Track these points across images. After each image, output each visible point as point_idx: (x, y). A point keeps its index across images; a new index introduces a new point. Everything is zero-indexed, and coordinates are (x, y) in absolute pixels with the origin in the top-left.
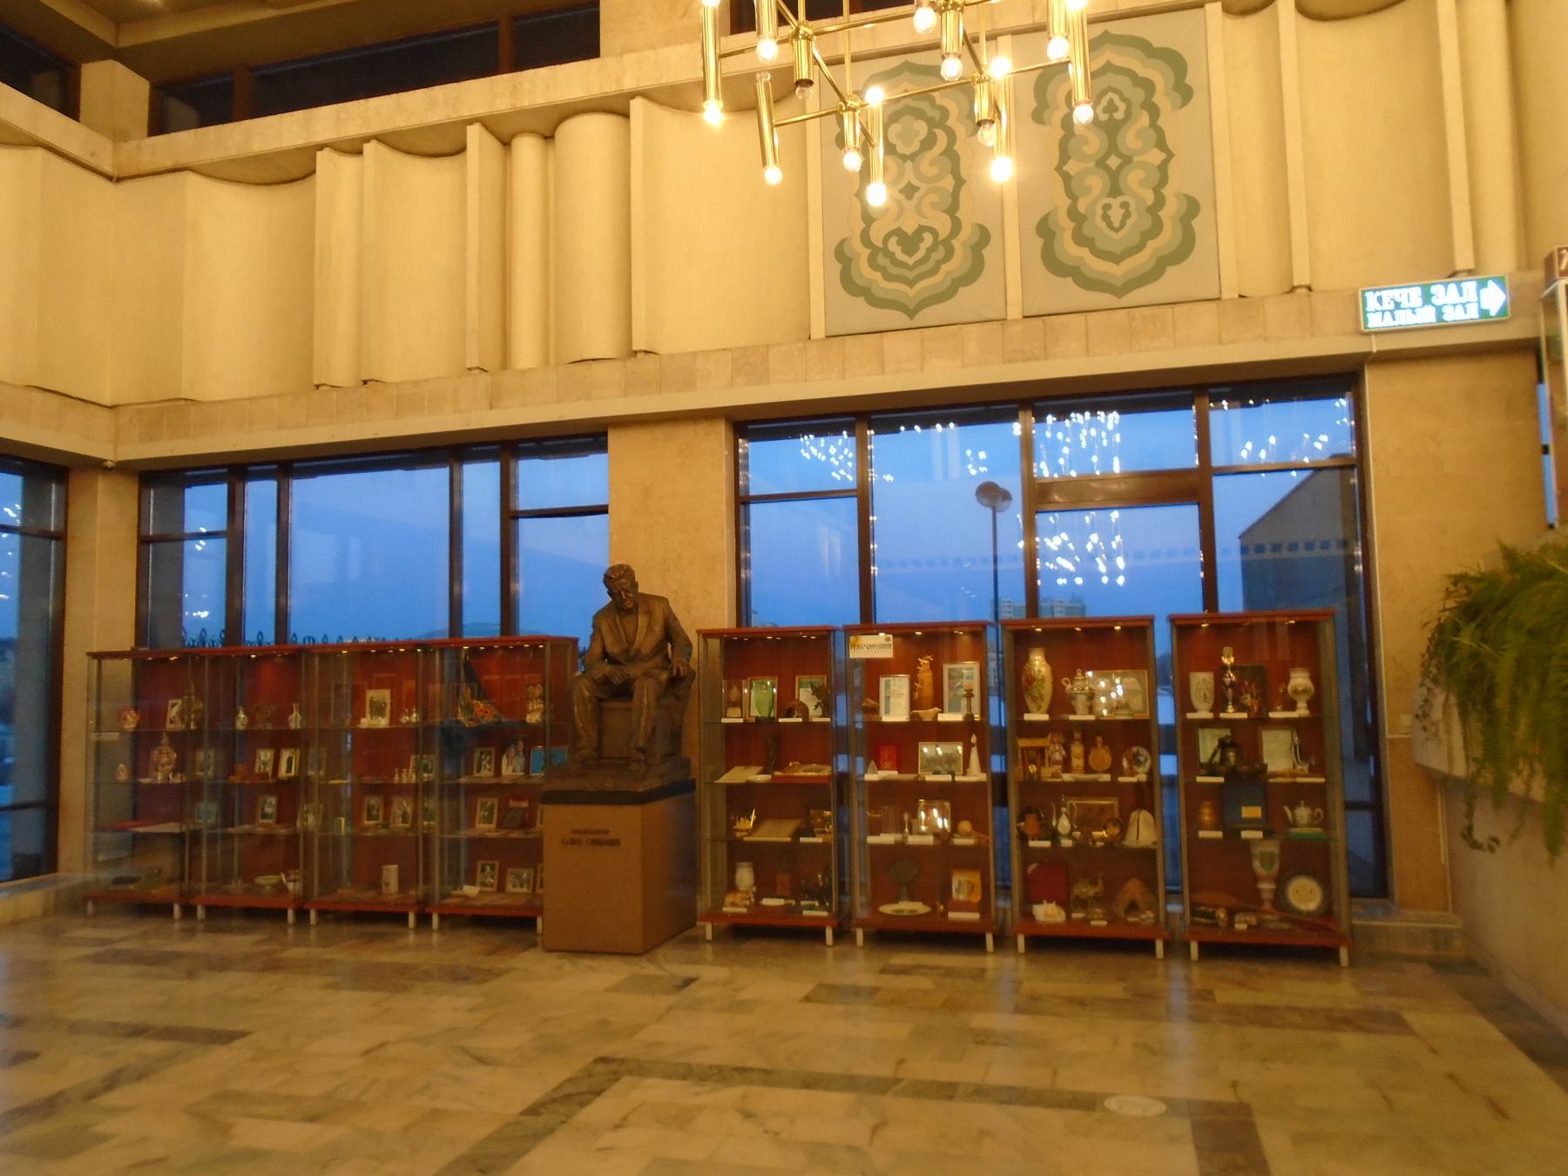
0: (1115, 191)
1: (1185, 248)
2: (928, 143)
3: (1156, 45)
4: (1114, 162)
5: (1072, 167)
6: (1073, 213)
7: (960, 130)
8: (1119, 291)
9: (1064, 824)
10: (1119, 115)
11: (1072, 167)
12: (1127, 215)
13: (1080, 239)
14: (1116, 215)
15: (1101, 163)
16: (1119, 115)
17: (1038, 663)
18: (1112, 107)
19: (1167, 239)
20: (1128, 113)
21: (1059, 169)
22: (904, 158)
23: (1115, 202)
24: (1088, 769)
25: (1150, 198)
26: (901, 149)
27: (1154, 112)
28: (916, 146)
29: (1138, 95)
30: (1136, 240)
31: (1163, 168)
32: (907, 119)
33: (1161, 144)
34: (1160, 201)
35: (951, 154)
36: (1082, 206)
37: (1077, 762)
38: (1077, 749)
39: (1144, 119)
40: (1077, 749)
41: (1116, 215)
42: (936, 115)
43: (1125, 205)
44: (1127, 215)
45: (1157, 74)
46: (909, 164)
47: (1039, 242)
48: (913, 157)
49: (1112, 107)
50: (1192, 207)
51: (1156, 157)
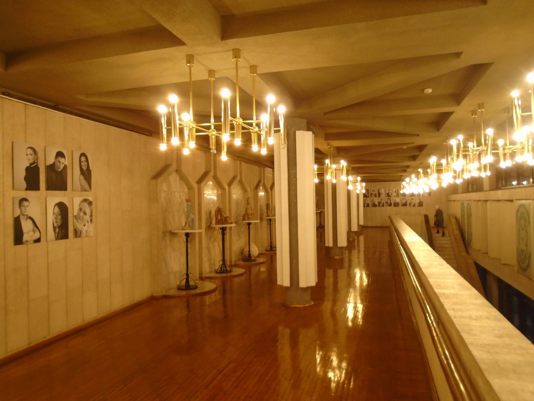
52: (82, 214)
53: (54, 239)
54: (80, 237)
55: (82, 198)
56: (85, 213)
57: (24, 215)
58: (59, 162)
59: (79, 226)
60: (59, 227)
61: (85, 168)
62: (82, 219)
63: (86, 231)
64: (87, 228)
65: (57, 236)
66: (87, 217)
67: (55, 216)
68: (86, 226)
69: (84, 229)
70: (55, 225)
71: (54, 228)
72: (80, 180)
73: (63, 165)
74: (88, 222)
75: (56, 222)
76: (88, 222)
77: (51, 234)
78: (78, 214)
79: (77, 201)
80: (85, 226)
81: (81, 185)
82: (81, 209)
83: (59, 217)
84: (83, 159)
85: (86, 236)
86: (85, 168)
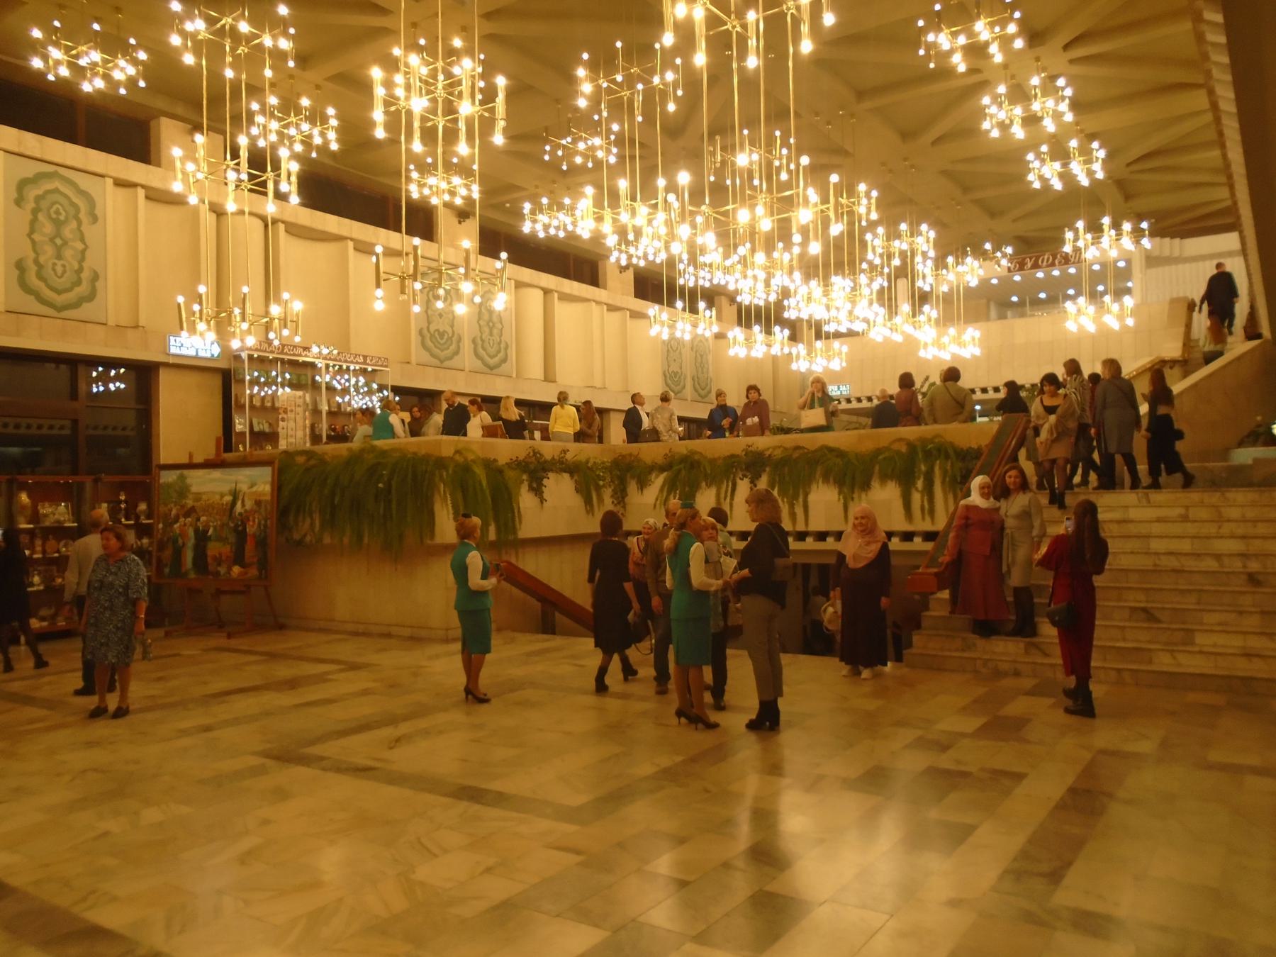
0: (59, 257)
1: (91, 297)
4: (59, 241)
5: (36, 237)
6: (36, 262)
8: (60, 309)
9: (36, 579)
11: (36, 237)
12: (64, 272)
13: (40, 277)
14: (59, 269)
15: (52, 240)
16: (62, 218)
17: (24, 497)
19: (83, 289)
20: (67, 218)
21: (29, 235)
23: (59, 263)
24: (44, 552)
25: (76, 266)
27: (80, 223)
29: (72, 211)
30: (68, 285)
31: (83, 252)
33: (82, 240)
34: (80, 270)
36: (42, 259)
37: (39, 549)
38: (38, 542)
39: (74, 224)
40: (38, 542)
41: (59, 269)
43: (64, 266)
44: (64, 272)
47: (17, 272)
49: (58, 212)
50: (95, 277)
51: (80, 246)
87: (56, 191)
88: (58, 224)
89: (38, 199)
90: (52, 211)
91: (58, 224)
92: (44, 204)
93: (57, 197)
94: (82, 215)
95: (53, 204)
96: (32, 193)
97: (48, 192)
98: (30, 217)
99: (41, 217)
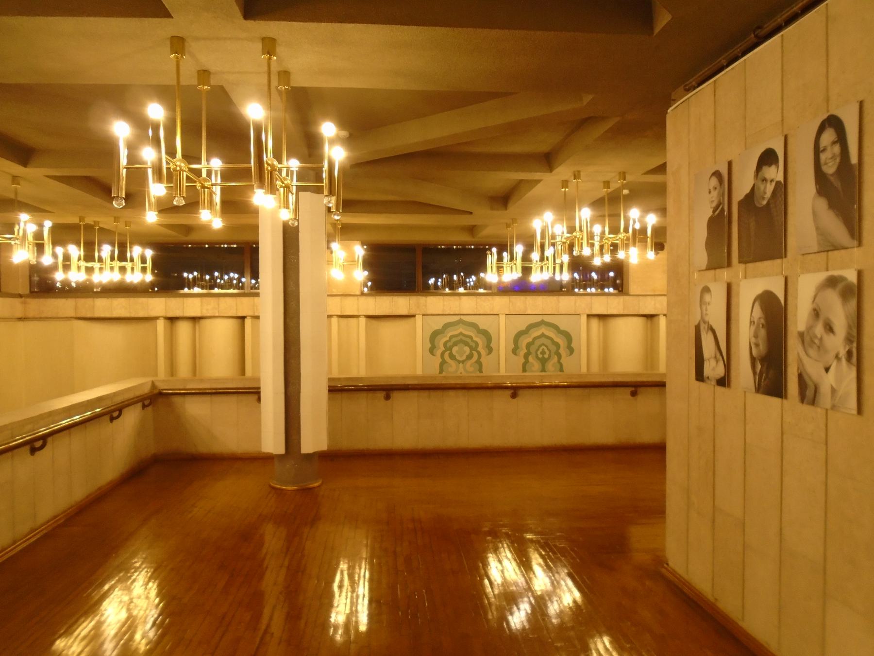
2: (470, 357)
3: (562, 328)
7: (483, 352)
10: (546, 356)
16: (546, 356)
18: (543, 353)
20: (550, 356)
22: (459, 362)
26: (458, 358)
28: (464, 357)
29: (553, 348)
32: (461, 345)
35: (479, 363)
39: (556, 358)
42: (474, 345)
45: (561, 340)
46: (461, 365)
48: (463, 362)
49: (543, 353)
52: (819, 330)
53: (754, 389)
54: (813, 402)
55: (822, 276)
56: (829, 328)
57: (705, 322)
58: (764, 180)
59: (813, 370)
60: (763, 360)
61: (830, 169)
62: (821, 347)
63: (834, 391)
64: (837, 380)
65: (759, 385)
66: (837, 343)
67: (753, 328)
68: (832, 370)
69: (828, 381)
70: (755, 352)
71: (753, 360)
72: (814, 213)
73: (774, 184)
74: (837, 357)
75: (757, 345)
76: (837, 357)
77: (744, 372)
78: (810, 328)
79: (807, 286)
80: (827, 370)
81: (820, 231)
82: (816, 313)
83: (763, 333)
84: (829, 136)
85: (834, 407)
86: (830, 169)
87: (543, 335)
88: (543, 362)
89: (529, 345)
90: (539, 353)
91: (543, 362)
92: (533, 349)
93: (543, 340)
94: (563, 351)
95: (540, 346)
96: (525, 341)
97: (535, 339)
98: (523, 360)
99: (530, 359)
